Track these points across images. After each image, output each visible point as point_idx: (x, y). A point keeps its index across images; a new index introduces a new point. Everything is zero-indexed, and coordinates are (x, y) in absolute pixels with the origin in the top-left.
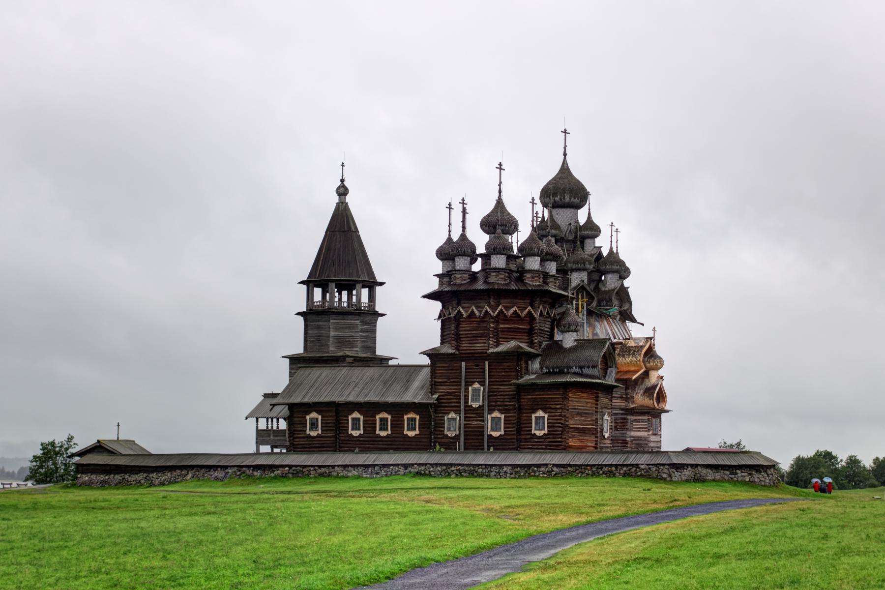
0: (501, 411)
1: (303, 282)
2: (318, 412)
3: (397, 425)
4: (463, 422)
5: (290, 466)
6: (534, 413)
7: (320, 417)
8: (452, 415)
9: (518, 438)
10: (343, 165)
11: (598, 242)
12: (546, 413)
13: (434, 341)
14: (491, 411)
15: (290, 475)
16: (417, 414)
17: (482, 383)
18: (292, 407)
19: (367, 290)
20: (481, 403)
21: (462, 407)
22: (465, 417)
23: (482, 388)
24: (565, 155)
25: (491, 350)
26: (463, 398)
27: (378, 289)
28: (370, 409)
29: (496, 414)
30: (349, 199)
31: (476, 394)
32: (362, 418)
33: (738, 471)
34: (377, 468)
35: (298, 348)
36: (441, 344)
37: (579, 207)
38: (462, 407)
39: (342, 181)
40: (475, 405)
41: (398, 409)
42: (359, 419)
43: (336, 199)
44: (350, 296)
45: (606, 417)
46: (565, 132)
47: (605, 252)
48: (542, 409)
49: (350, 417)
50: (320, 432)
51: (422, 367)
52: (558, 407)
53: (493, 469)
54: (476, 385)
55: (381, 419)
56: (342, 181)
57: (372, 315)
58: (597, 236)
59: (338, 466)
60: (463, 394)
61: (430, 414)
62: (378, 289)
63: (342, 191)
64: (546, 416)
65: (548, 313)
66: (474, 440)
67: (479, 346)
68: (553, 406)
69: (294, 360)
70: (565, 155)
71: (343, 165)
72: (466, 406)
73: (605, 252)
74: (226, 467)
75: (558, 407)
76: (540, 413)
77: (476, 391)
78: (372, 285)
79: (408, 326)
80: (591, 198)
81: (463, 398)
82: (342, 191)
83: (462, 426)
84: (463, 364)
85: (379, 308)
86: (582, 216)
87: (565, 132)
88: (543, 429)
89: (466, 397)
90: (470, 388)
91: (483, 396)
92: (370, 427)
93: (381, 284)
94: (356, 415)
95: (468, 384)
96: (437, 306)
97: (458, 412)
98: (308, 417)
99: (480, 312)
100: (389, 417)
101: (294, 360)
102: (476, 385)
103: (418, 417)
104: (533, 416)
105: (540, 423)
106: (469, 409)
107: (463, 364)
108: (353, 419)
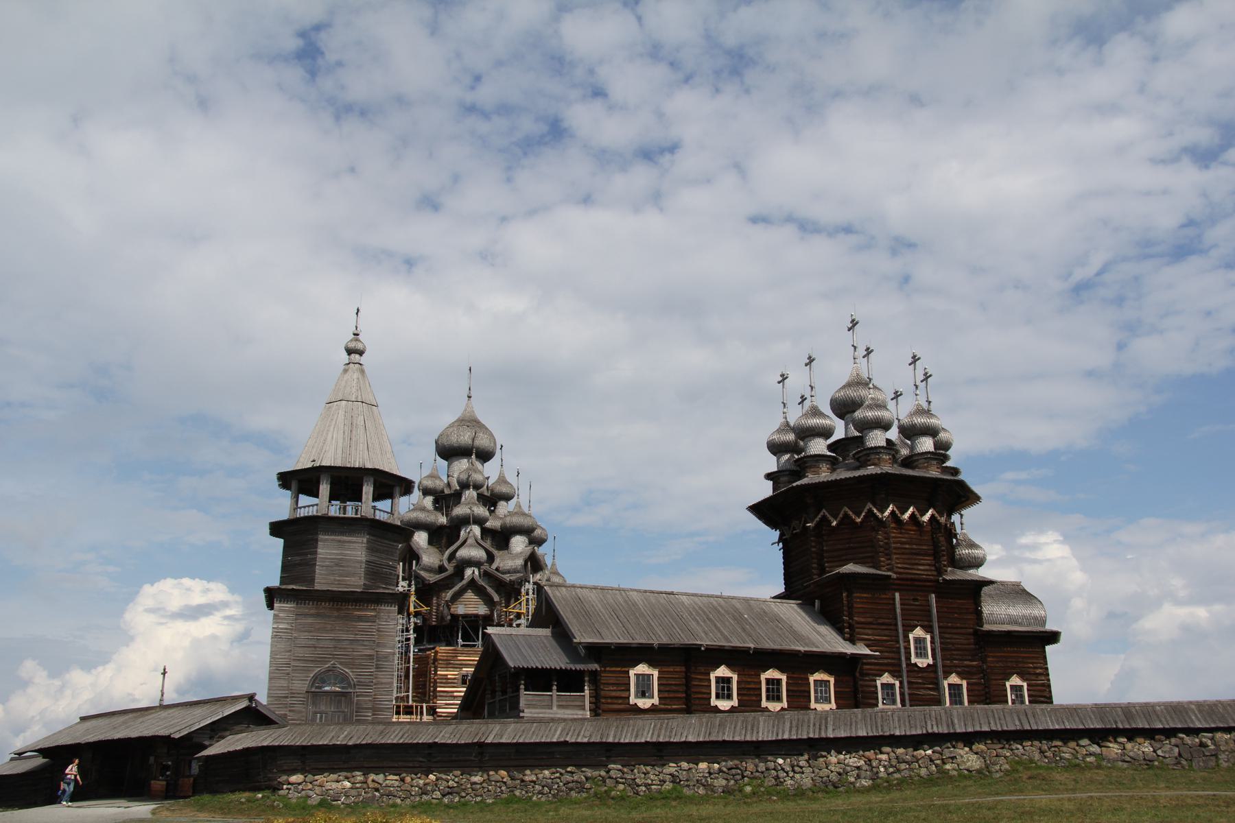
0: (961, 675)
2: (652, 664)
4: (906, 691)
7: (656, 673)
8: (886, 678)
12: (1024, 680)
14: (947, 674)
16: (830, 674)
17: (928, 629)
20: (930, 661)
21: (904, 665)
22: (909, 683)
26: (903, 650)
28: (750, 661)
29: (954, 679)
32: (735, 677)
38: (904, 665)
40: (922, 663)
42: (729, 680)
49: (713, 676)
50: (656, 701)
54: (918, 632)
55: (768, 681)
60: (902, 644)
68: (1031, 671)
72: (909, 664)
74: (1170, 733)
77: (919, 641)
81: (903, 650)
83: (907, 697)
84: (897, 595)
89: (908, 649)
90: (911, 636)
91: (933, 650)
94: (723, 671)
97: (896, 673)
98: (632, 673)
100: (784, 678)
102: (918, 632)
103: (832, 680)
104: (1008, 684)
107: (897, 595)
108: (718, 679)
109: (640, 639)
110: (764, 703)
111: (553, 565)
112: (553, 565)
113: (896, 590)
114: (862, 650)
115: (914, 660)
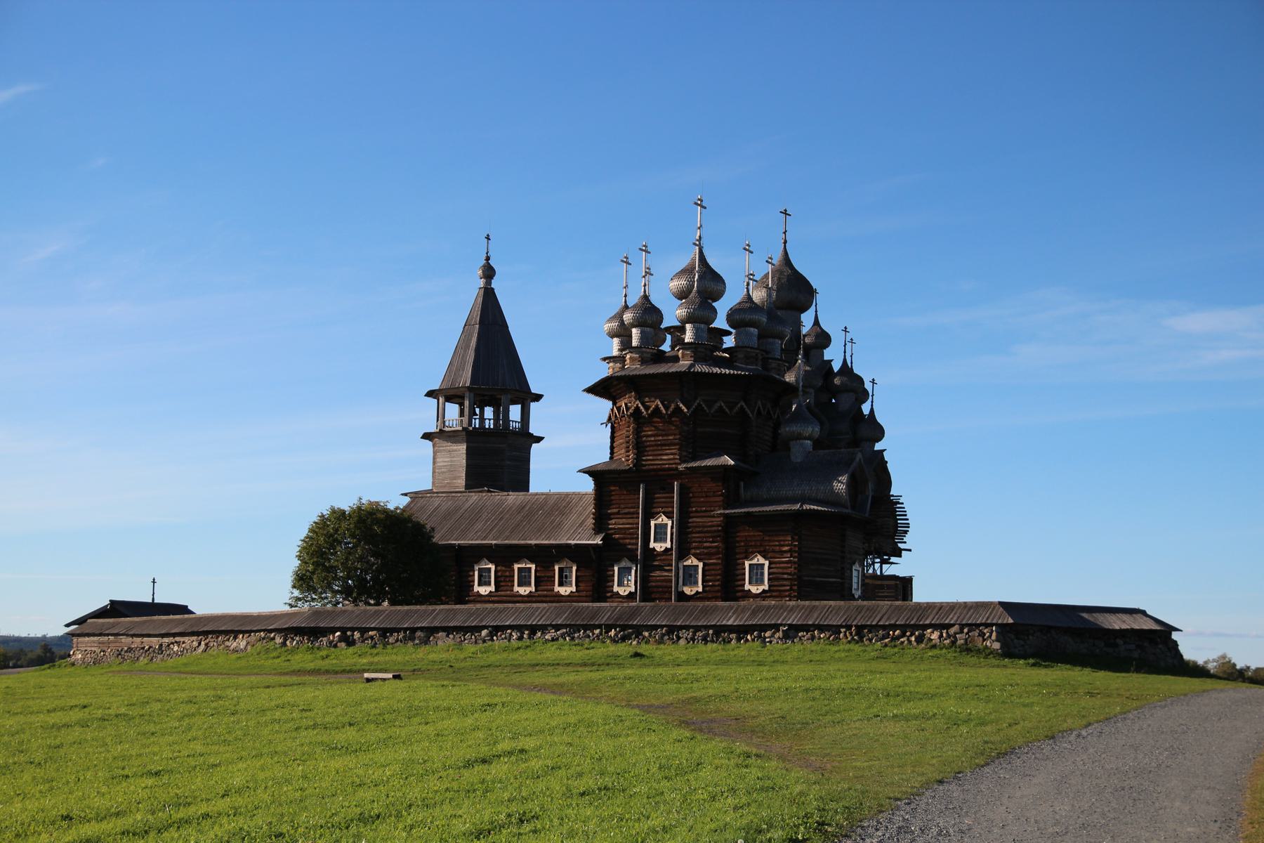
1: (430, 394)
3: (543, 580)
5: (343, 630)
6: (747, 558)
10: (488, 238)
11: (828, 354)
12: (765, 558)
13: (600, 455)
14: (682, 555)
15: (343, 645)
17: (669, 516)
19: (519, 406)
20: (668, 545)
23: (670, 523)
24: (785, 242)
25: (681, 467)
27: (533, 405)
28: (505, 556)
33: (1119, 641)
34: (484, 632)
36: (611, 458)
37: (805, 308)
39: (488, 259)
40: (659, 547)
41: (545, 556)
43: (482, 283)
44: (496, 413)
45: (856, 567)
46: (785, 213)
47: (836, 367)
48: (760, 553)
51: (581, 496)
52: (786, 548)
53: (683, 633)
56: (488, 259)
57: (526, 439)
58: (827, 346)
59: (422, 629)
61: (594, 566)
62: (533, 405)
63: (489, 272)
64: (767, 563)
65: (769, 412)
67: (668, 458)
70: (785, 242)
71: (488, 238)
73: (836, 367)
74: (250, 632)
75: (786, 548)
76: (759, 559)
78: (527, 397)
79: (570, 443)
80: (819, 298)
82: (489, 272)
85: (534, 429)
86: (807, 319)
87: (785, 213)
88: (762, 582)
90: (653, 523)
92: (503, 582)
93: (538, 397)
95: (649, 515)
96: (609, 404)
99: (667, 408)
102: (663, 519)
104: (747, 564)
105: (757, 574)
106: (649, 553)
110: (516, 588)
111: (872, 411)
112: (872, 411)
113: (642, 482)
115: (652, 545)
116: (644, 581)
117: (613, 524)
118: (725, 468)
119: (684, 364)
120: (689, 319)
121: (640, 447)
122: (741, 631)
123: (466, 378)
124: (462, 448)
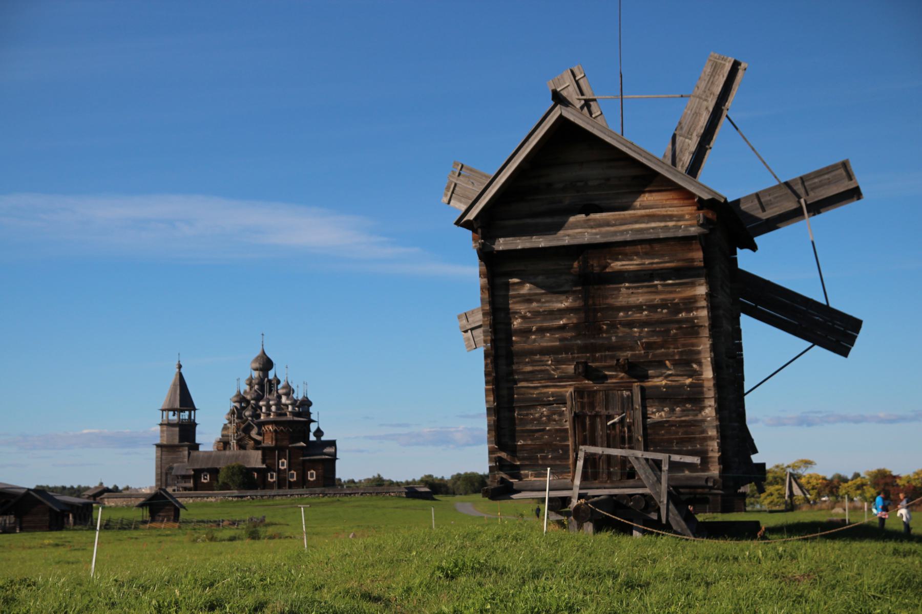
9: (303, 482)
14: (290, 470)
18: (194, 470)
30: (182, 370)
31: (283, 464)
35: (158, 441)
40: (282, 468)
61: (262, 472)
63: (180, 367)
66: (282, 483)
67: (285, 443)
69: (158, 446)
82: (180, 367)
85: (197, 421)
86: (271, 375)
95: (279, 459)
101: (158, 446)
106: (279, 470)
109: (203, 467)
114: (264, 466)
116: (278, 477)
117: (268, 461)
118: (303, 447)
119: (289, 417)
120: (291, 404)
121: (276, 440)
122: (350, 494)
123: (177, 405)
124: (177, 429)
